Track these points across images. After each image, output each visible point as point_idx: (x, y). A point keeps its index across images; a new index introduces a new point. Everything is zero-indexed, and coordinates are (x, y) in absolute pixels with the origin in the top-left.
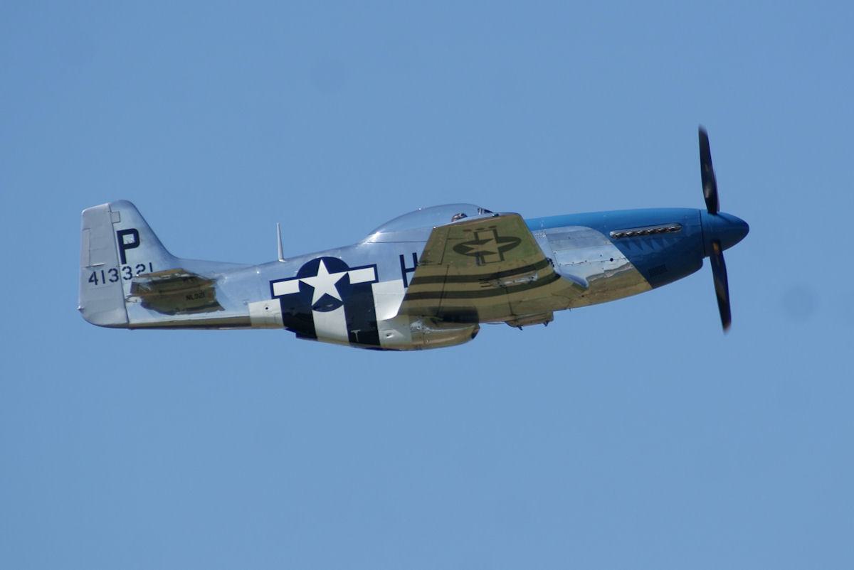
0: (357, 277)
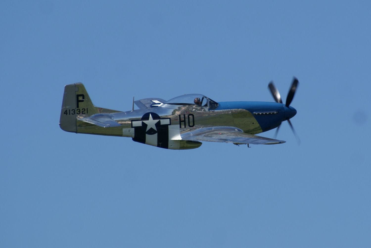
0: (163, 122)
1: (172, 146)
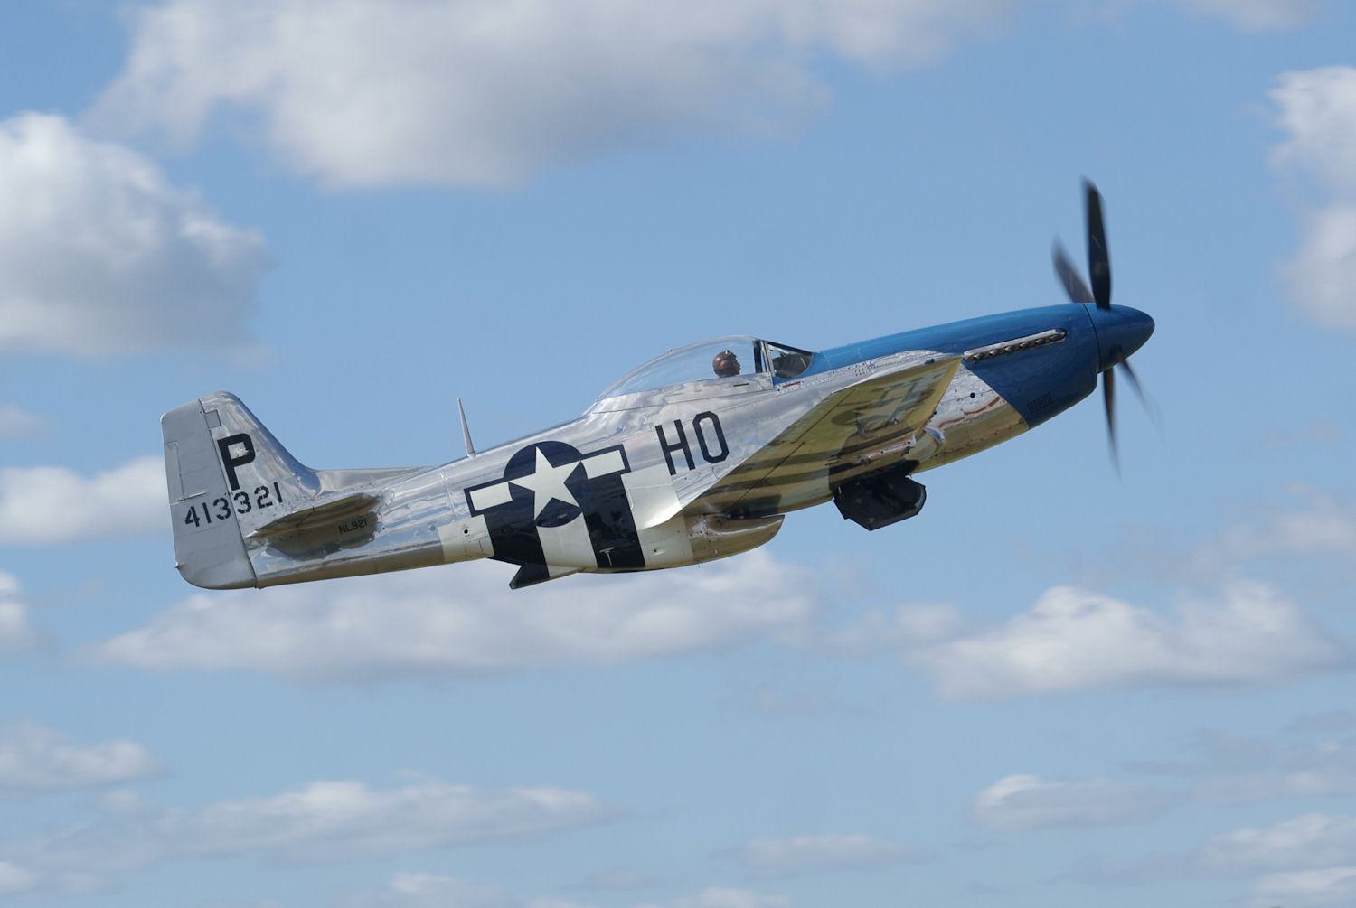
0: (596, 468)
1: (657, 554)
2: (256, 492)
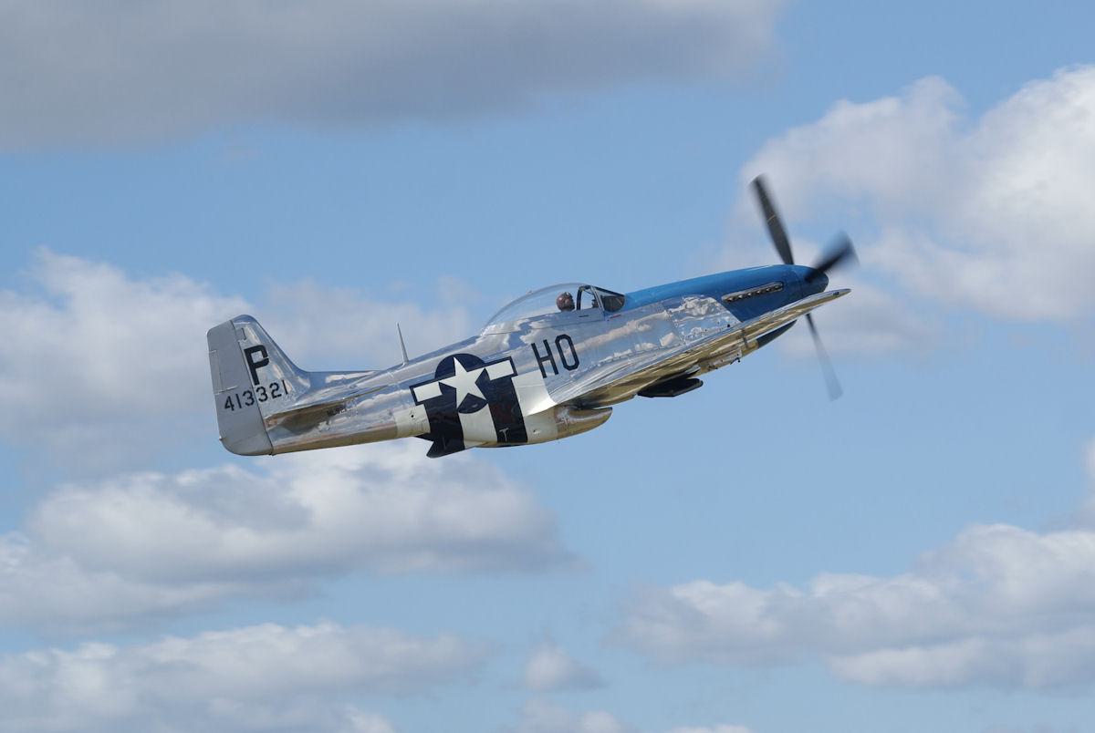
0: (496, 372)
2: (271, 387)
